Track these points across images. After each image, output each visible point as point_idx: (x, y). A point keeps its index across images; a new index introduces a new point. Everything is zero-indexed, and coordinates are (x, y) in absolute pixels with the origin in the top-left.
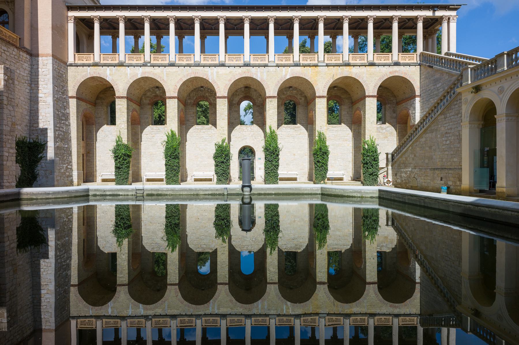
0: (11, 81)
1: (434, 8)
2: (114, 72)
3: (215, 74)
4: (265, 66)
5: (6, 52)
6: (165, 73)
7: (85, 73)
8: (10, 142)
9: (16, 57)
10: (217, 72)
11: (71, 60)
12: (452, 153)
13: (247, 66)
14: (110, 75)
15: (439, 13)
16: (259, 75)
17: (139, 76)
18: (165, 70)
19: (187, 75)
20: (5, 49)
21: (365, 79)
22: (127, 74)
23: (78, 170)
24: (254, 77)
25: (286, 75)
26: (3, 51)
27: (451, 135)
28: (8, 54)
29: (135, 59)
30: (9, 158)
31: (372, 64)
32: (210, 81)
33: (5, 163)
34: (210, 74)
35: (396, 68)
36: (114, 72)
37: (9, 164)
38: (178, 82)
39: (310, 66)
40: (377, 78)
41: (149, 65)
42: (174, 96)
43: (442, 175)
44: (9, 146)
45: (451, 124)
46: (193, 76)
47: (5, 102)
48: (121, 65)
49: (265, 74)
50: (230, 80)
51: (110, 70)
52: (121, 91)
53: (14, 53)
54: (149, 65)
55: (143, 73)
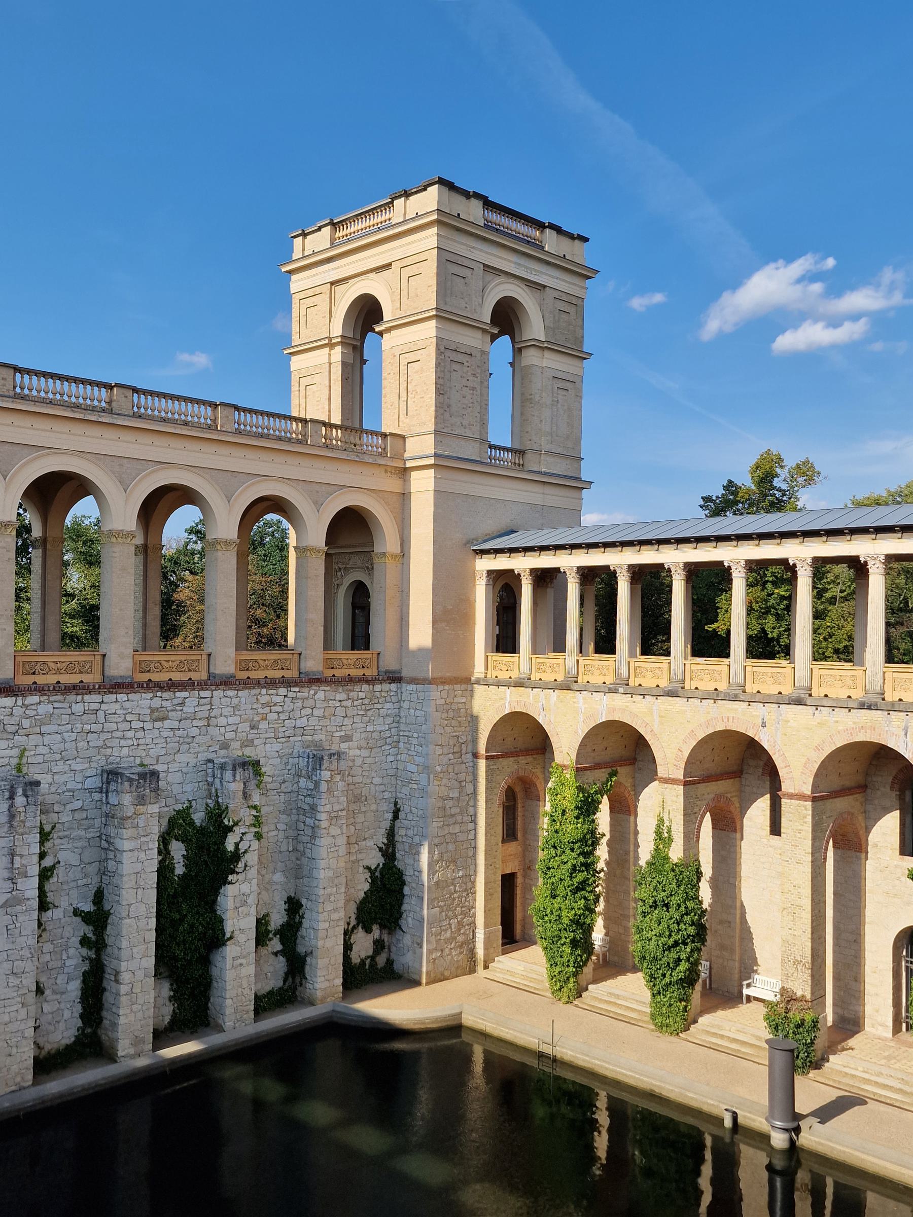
0: (338, 778)
5: (344, 703)
8: (332, 899)
9: (366, 701)
11: (479, 671)
19: (708, 723)
20: (343, 696)
23: (486, 926)
26: (338, 704)
28: (349, 703)
30: (331, 932)
33: (320, 943)
37: (329, 943)
38: (685, 742)
44: (329, 907)
47: (324, 824)
50: (817, 748)
52: (565, 750)
53: (362, 695)
54: (621, 690)
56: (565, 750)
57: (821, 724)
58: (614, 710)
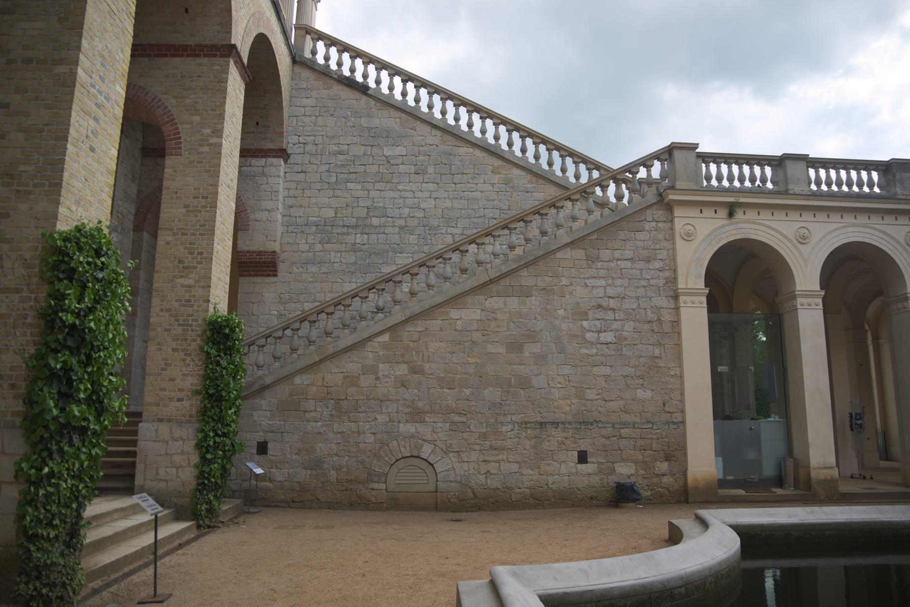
12: (629, 370)
27: (620, 315)
43: (584, 446)
45: (618, 282)
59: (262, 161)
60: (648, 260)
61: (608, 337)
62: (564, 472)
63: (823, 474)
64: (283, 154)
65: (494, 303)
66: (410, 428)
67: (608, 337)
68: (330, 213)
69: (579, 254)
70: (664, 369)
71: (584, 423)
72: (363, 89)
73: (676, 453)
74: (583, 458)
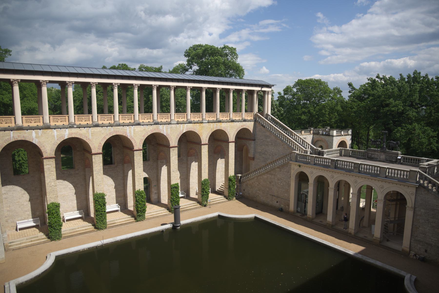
1: (262, 86)
2: (40, 135)
3: (132, 131)
4: (170, 124)
6: (90, 132)
7: (7, 137)
10: (134, 130)
13: (157, 124)
14: (36, 137)
15: (264, 89)
16: (165, 131)
17: (66, 138)
18: (90, 131)
19: (110, 133)
21: (229, 130)
22: (54, 136)
24: (162, 132)
25: (183, 130)
29: (59, 121)
31: (233, 121)
32: (129, 137)
34: (128, 132)
35: (244, 123)
36: (40, 135)
38: (102, 140)
39: (198, 123)
40: (235, 130)
41: (75, 126)
42: (99, 152)
46: (114, 134)
48: (47, 127)
49: (169, 130)
50: (143, 136)
51: (36, 133)
52: (49, 152)
55: (69, 134)
56: (49, 152)
57: (144, 130)
58: (72, 134)
59: (250, 141)
60: (288, 172)
61: (282, 184)
62: (274, 203)
63: (309, 216)
64: (254, 140)
65: (268, 175)
66: (258, 192)
67: (282, 184)
68: (260, 151)
69: (279, 169)
70: (288, 191)
71: (278, 197)
72: (264, 127)
73: (289, 205)
74: (277, 202)
